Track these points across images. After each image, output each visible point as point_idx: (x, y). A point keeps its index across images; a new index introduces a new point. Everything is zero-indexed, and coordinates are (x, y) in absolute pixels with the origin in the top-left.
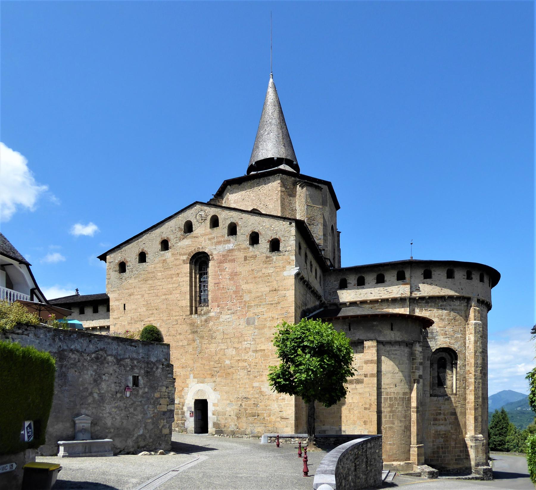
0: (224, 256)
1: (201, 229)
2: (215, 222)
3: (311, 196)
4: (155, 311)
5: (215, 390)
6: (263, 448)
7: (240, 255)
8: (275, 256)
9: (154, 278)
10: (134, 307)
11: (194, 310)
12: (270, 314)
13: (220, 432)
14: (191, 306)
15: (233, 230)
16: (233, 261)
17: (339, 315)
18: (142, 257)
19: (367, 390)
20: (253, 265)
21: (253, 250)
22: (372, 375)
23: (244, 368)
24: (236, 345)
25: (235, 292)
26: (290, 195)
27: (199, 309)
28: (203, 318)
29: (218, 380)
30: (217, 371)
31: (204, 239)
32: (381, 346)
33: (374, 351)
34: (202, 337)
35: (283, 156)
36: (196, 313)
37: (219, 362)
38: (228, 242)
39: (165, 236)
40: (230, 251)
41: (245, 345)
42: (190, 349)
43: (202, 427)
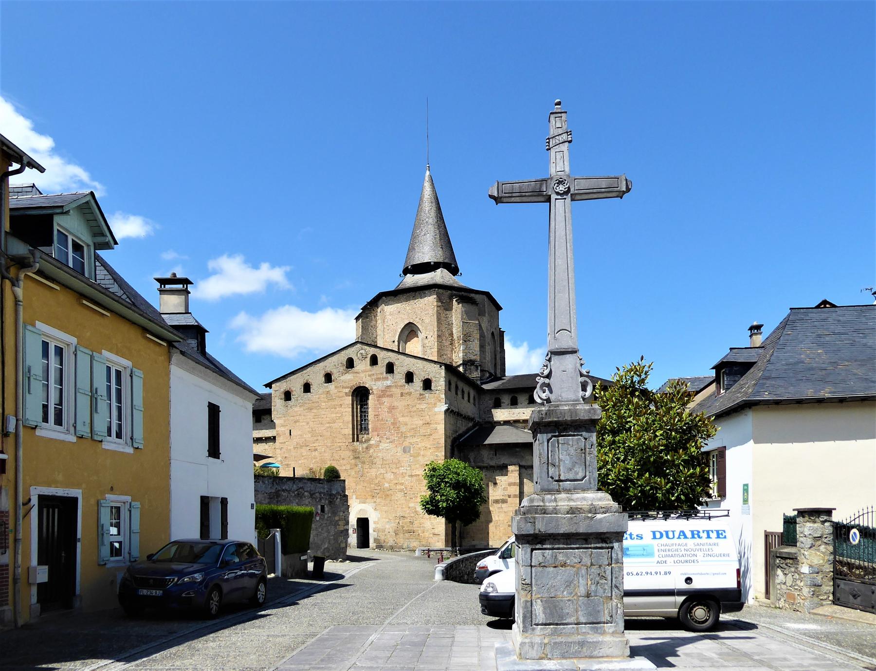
0: (382, 391)
1: (362, 365)
2: (374, 361)
3: (467, 313)
4: (319, 438)
5: (375, 509)
6: (418, 558)
7: (397, 391)
8: (427, 394)
9: (319, 407)
10: (299, 433)
11: (356, 438)
12: (423, 444)
13: (380, 547)
14: (353, 434)
15: (390, 368)
16: (391, 396)
17: (486, 442)
18: (307, 388)
19: (511, 509)
21: (408, 388)
22: (515, 496)
24: (394, 470)
25: (393, 424)
26: (447, 310)
28: (365, 445)
29: (378, 500)
30: (378, 493)
31: (363, 375)
32: (523, 470)
33: (517, 474)
34: (364, 463)
35: (441, 260)
36: (358, 441)
37: (378, 484)
38: (387, 379)
39: (328, 370)
40: (388, 387)
41: (402, 470)
42: (353, 473)
43: (364, 542)
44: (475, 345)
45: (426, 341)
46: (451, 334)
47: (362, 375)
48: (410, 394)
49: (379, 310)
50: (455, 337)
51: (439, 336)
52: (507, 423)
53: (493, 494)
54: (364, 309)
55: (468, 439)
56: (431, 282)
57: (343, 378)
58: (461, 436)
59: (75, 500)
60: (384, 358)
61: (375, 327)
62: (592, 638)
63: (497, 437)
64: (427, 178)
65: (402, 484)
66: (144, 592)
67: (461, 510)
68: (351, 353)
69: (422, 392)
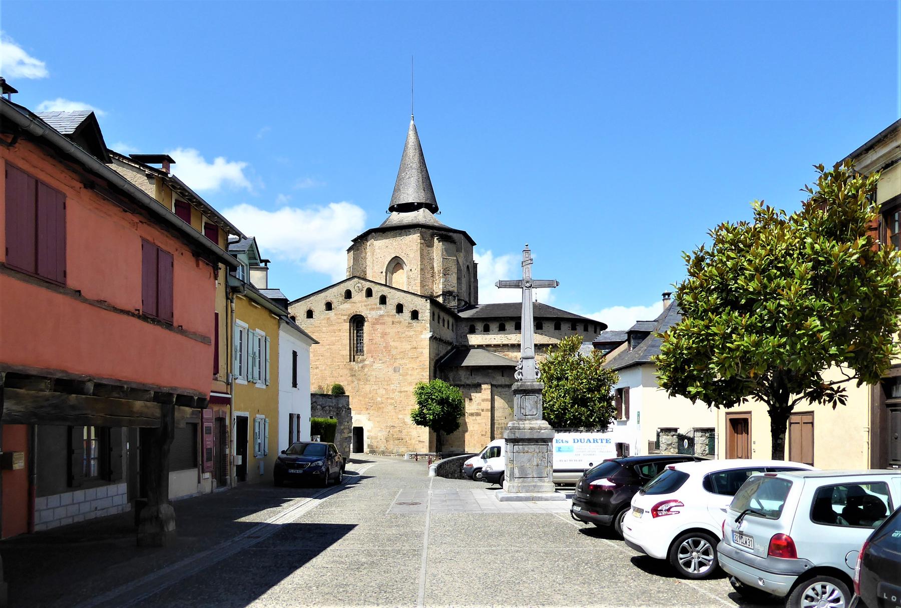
1: (359, 297)
2: (369, 293)
6: (407, 461)
7: (390, 320)
8: (414, 323)
11: (352, 359)
13: (373, 452)
15: (383, 300)
16: (384, 324)
20: (398, 328)
21: (398, 317)
22: (487, 410)
23: (391, 404)
25: (385, 347)
26: (429, 246)
27: (356, 357)
28: (360, 365)
29: (372, 412)
31: (359, 304)
32: (494, 388)
33: (489, 392)
34: (359, 380)
35: (423, 201)
37: (372, 399)
40: (381, 316)
41: (392, 387)
43: (359, 449)
44: (453, 278)
46: (433, 268)
47: (359, 305)
48: (400, 322)
49: (368, 244)
50: (436, 270)
51: (422, 269)
52: (480, 347)
53: (469, 407)
54: (355, 241)
55: (448, 361)
56: (415, 222)
57: (341, 307)
58: (442, 358)
59: (246, 418)
60: (378, 291)
61: (365, 258)
62: (539, 484)
63: (473, 359)
64: (411, 127)
65: (392, 399)
66: (292, 471)
67: (443, 422)
68: (349, 285)
69: (411, 321)
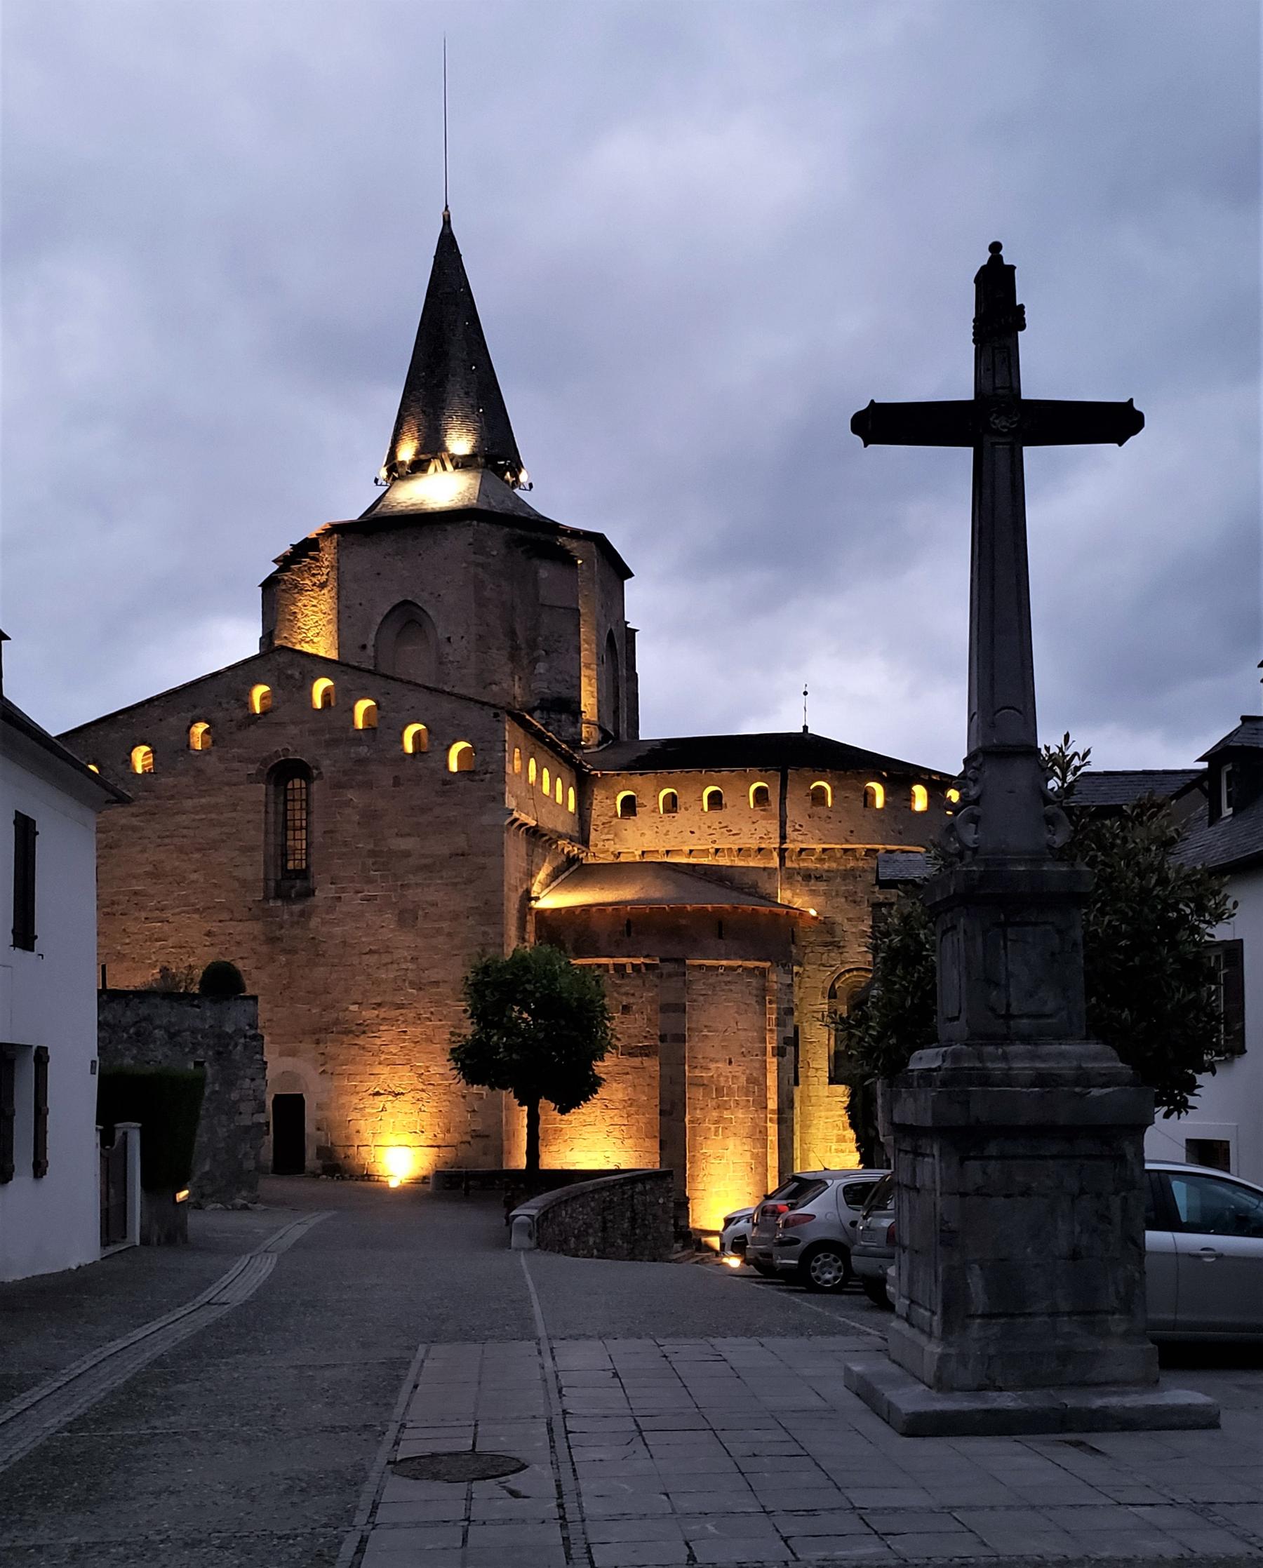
34: (293, 951)
45: (447, 649)
